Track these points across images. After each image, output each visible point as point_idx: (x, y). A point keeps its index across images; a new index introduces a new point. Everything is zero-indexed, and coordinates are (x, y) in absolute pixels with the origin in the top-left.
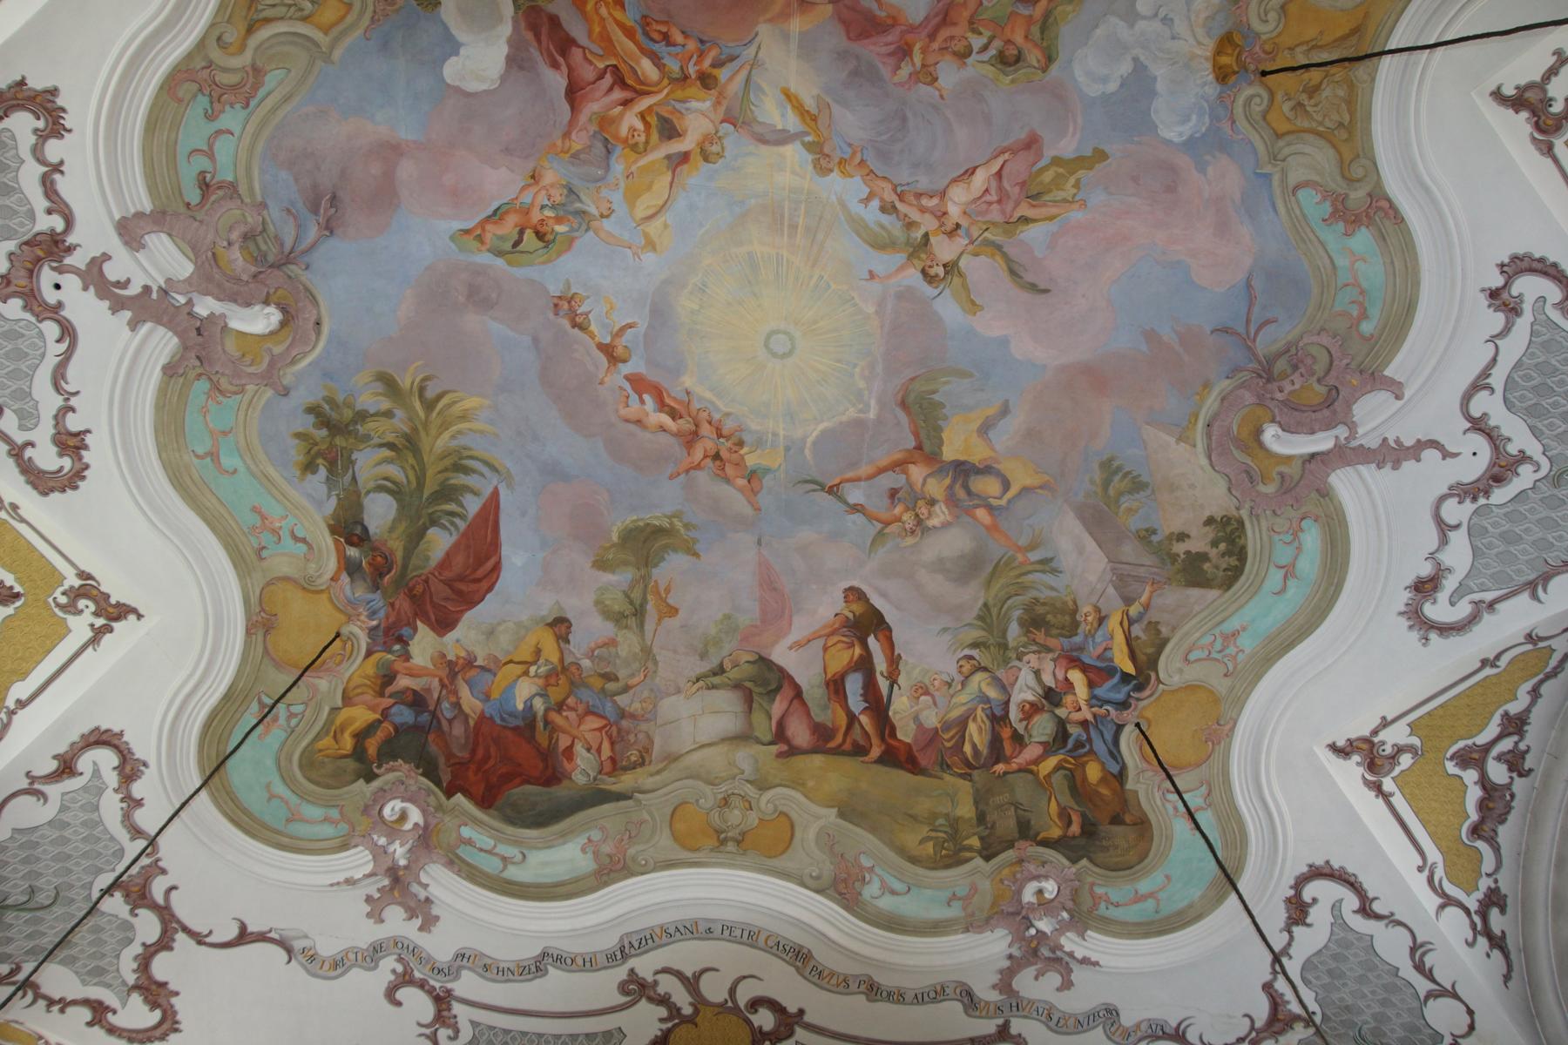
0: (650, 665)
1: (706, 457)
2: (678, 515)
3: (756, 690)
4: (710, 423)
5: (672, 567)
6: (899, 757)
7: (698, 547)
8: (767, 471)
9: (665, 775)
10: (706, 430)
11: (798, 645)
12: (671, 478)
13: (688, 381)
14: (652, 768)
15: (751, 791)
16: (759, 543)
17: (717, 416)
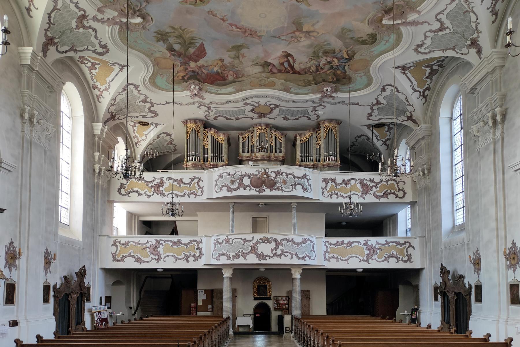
0: (242, 64)
1: (248, 34)
2: (244, 43)
3: (265, 66)
4: (249, 29)
5: (244, 51)
6: (295, 72)
7: (249, 47)
8: (263, 36)
9: (247, 78)
10: (248, 30)
11: (273, 59)
12: (241, 38)
13: (242, 23)
14: (245, 77)
15: (266, 79)
16: (262, 46)
17: (250, 28)
